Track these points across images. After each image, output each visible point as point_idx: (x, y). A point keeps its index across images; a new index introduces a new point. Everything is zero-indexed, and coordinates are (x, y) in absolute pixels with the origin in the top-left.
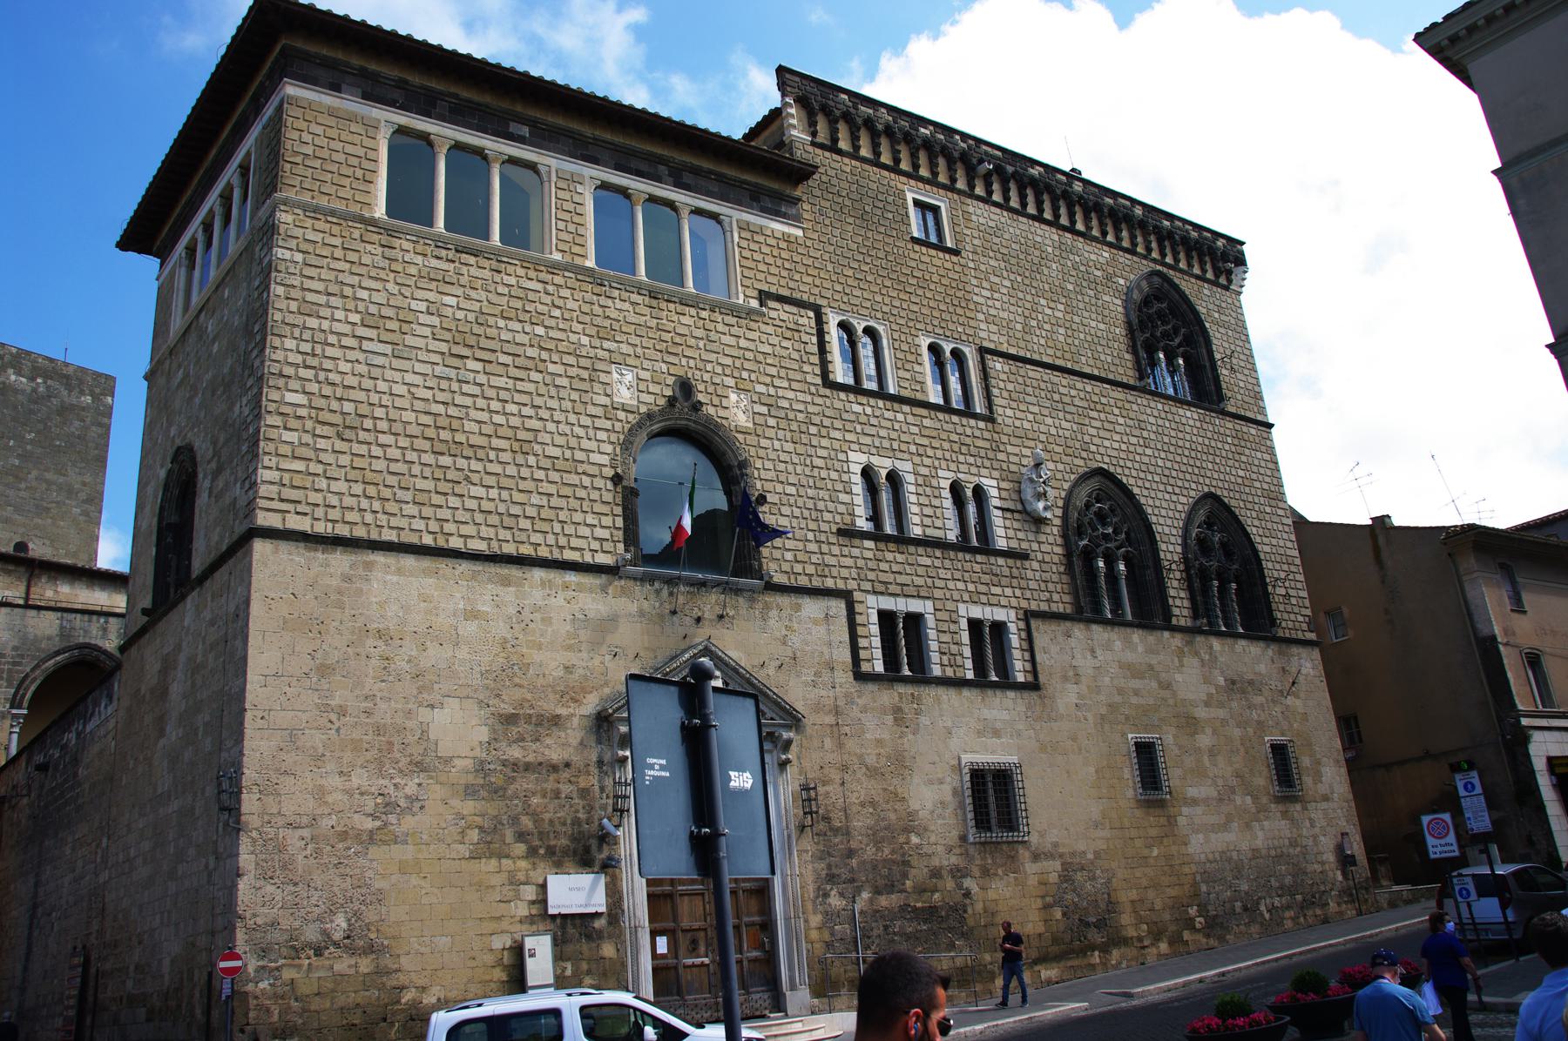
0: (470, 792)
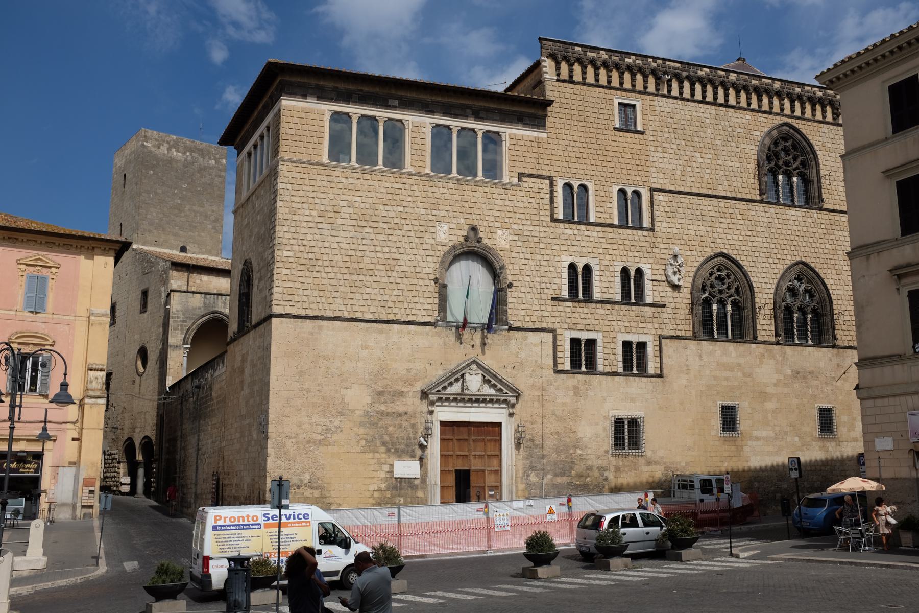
0: (362, 424)
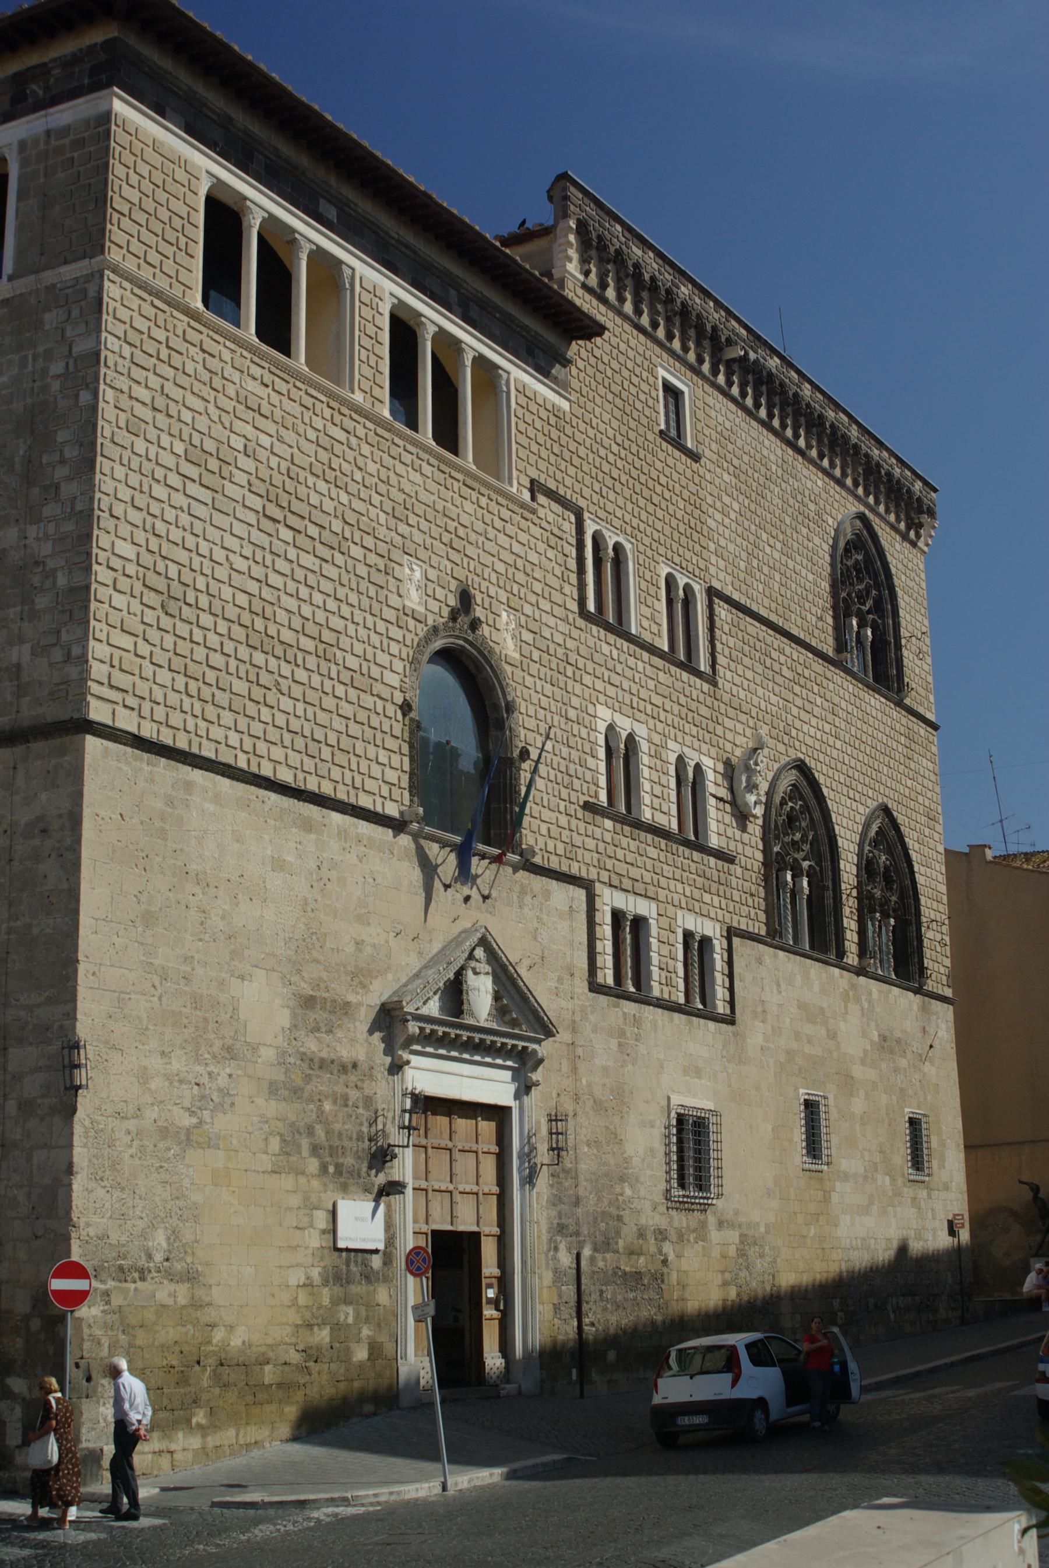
0: (273, 1089)
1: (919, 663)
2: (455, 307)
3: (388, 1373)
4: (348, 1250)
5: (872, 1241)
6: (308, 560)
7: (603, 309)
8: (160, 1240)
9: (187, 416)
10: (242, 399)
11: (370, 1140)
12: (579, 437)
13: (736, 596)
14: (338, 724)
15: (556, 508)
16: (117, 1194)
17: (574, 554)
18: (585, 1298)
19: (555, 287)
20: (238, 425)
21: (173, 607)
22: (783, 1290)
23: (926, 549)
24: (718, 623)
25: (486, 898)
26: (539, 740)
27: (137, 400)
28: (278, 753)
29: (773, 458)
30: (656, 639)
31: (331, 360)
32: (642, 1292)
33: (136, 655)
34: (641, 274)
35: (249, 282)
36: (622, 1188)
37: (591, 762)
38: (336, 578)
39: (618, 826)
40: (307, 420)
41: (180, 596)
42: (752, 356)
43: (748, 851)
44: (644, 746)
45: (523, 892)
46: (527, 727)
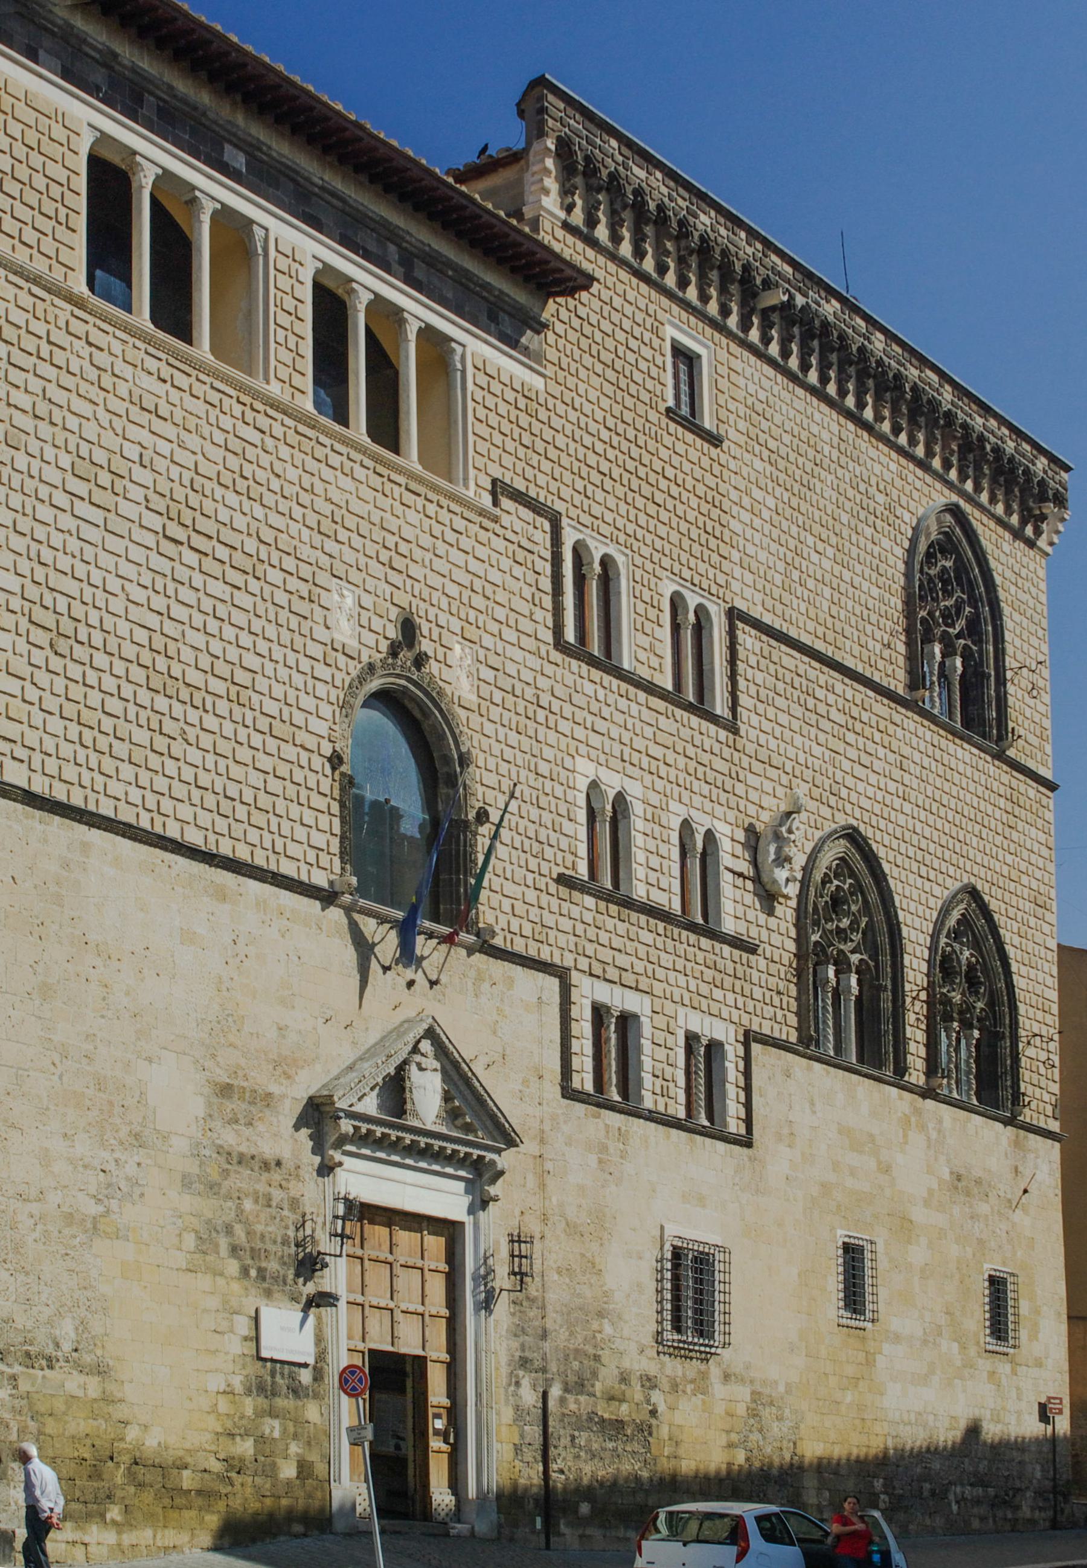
0: (186, 1182)
1: (1031, 702)
2: (395, 266)
3: (319, 1494)
4: (272, 1360)
5: (931, 1418)
6: (216, 588)
7: (590, 253)
8: (67, 1331)
9: (73, 423)
10: (136, 399)
11: (297, 1245)
12: (557, 423)
13: (767, 619)
14: (256, 778)
15: (526, 514)
16: (21, 1277)
17: (548, 572)
18: (553, 1441)
19: (527, 229)
20: (133, 432)
21: (63, 646)
22: (807, 1461)
23: (1049, 549)
24: (742, 654)
25: (433, 983)
26: (502, 800)
27: (16, 407)
28: (185, 812)
29: (825, 436)
30: (657, 674)
31: (239, 344)
32: (625, 1443)
33: (24, 701)
34: (644, 203)
35: (140, 256)
36: (601, 1325)
37: (568, 827)
38: (250, 608)
39: (602, 905)
40: (213, 420)
41: (71, 634)
42: (800, 301)
43: (776, 939)
44: (638, 808)
45: (479, 978)
46: (484, 785)
